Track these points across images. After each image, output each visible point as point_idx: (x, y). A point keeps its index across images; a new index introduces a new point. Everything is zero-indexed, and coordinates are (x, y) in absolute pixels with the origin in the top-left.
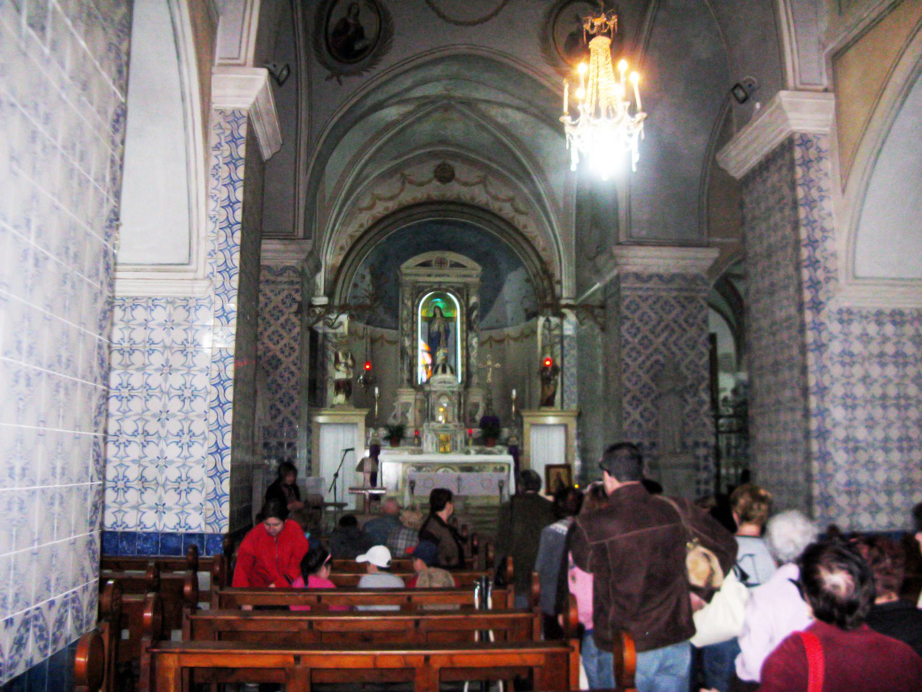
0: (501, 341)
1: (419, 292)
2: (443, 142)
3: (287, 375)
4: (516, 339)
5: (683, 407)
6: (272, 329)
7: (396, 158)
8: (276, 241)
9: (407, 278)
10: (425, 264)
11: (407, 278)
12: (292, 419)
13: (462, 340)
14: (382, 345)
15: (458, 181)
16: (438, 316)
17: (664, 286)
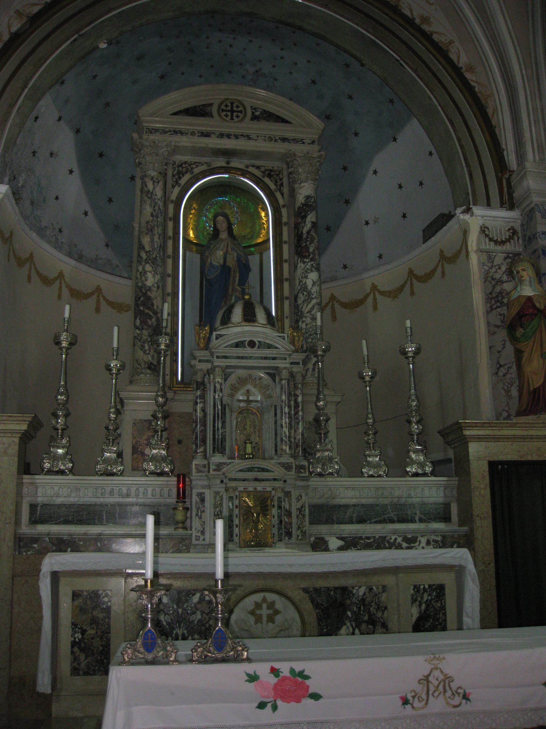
4: (394, 294)
16: (224, 235)
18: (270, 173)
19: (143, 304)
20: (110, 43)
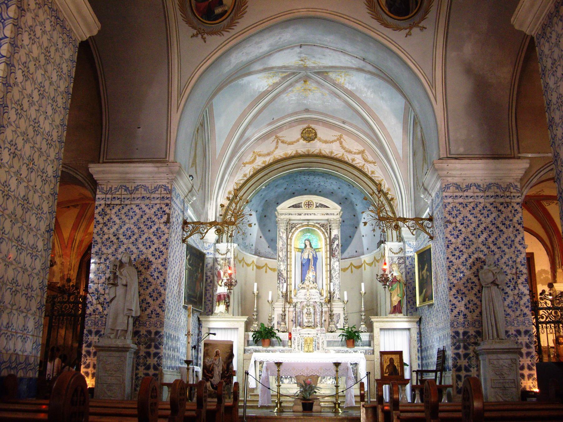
0: (360, 267)
1: (291, 227)
2: (307, 111)
3: (156, 274)
4: (370, 265)
5: (505, 299)
6: (146, 236)
7: (270, 124)
8: (150, 165)
9: (282, 217)
10: (295, 206)
11: (282, 217)
12: (159, 310)
13: (326, 265)
14: (266, 272)
15: (320, 140)
16: (308, 247)
17: (482, 194)
18: (323, 226)
19: (280, 276)
20: (266, 187)
